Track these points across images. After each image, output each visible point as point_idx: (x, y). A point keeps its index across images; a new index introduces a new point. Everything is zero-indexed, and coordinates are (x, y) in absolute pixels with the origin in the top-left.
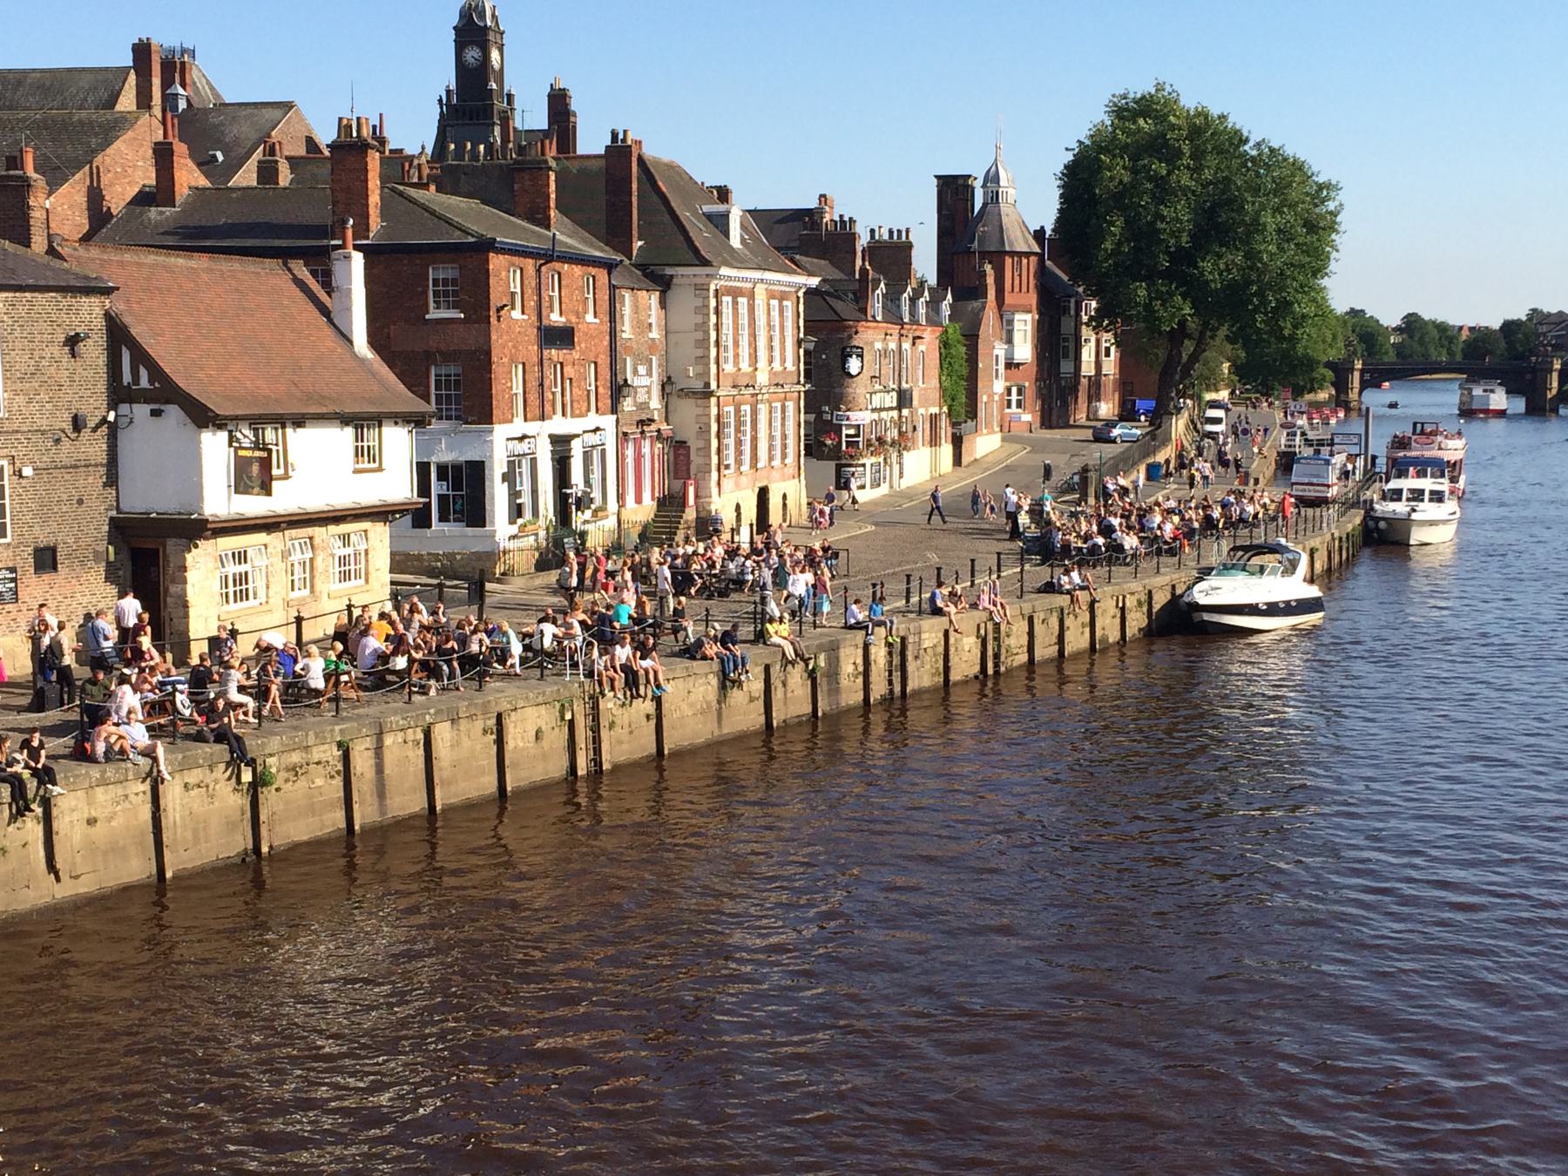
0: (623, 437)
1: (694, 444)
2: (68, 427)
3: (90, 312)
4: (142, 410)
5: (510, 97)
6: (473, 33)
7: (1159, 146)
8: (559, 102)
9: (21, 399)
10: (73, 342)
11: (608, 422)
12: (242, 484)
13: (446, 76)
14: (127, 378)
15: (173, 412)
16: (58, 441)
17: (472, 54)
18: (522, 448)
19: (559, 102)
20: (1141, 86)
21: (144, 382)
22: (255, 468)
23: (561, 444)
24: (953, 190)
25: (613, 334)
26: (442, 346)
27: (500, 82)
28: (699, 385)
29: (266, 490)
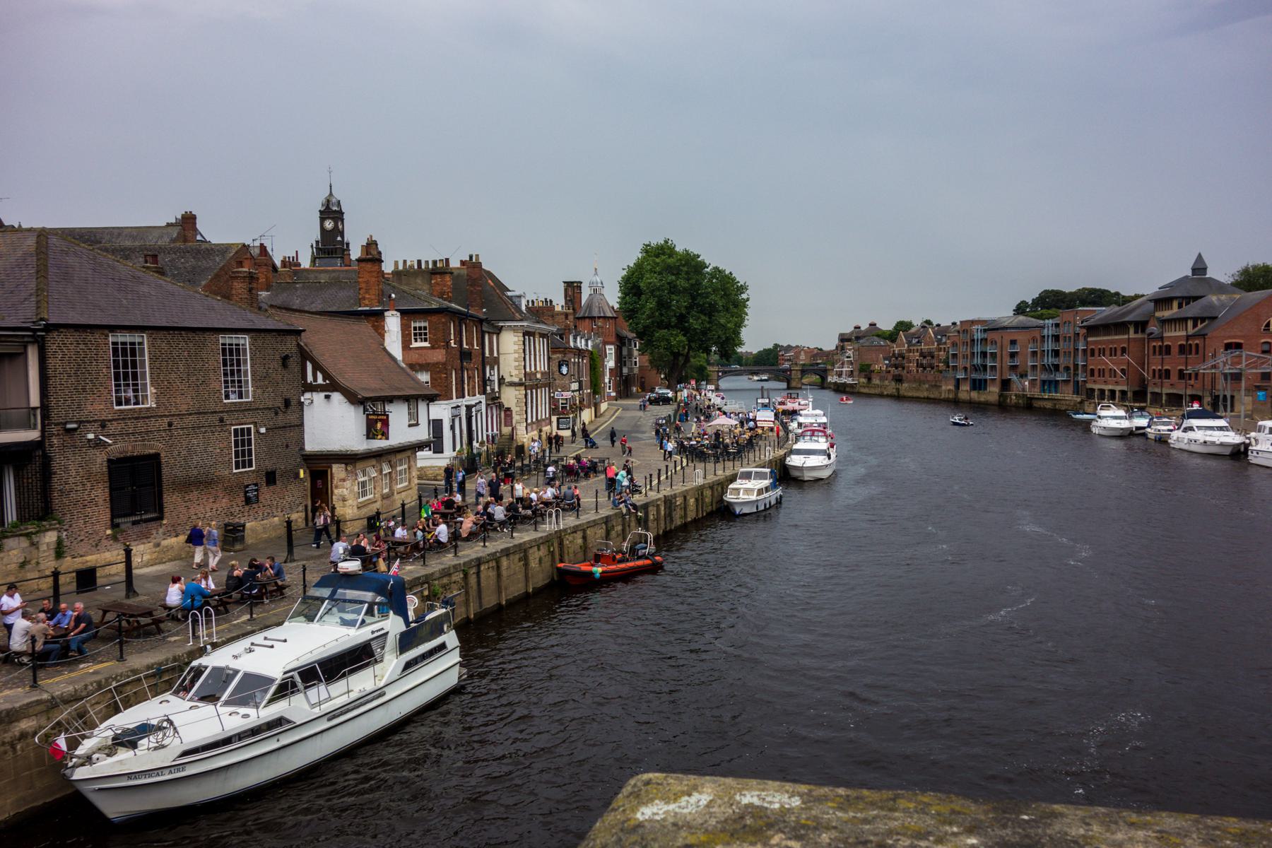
0: (487, 405)
1: (515, 409)
2: (282, 407)
3: (290, 345)
4: (318, 397)
5: (348, 244)
6: (332, 212)
7: (674, 270)
8: (371, 245)
9: (259, 391)
10: (285, 359)
11: (483, 398)
12: (371, 434)
13: (317, 235)
14: (310, 378)
15: (337, 397)
16: (276, 414)
17: (329, 225)
18: (456, 412)
19: (371, 245)
20: (657, 240)
21: (320, 380)
22: (379, 425)
23: (469, 408)
24: (572, 289)
25: (483, 353)
26: (420, 361)
27: (343, 237)
28: (516, 380)
29: (385, 435)
